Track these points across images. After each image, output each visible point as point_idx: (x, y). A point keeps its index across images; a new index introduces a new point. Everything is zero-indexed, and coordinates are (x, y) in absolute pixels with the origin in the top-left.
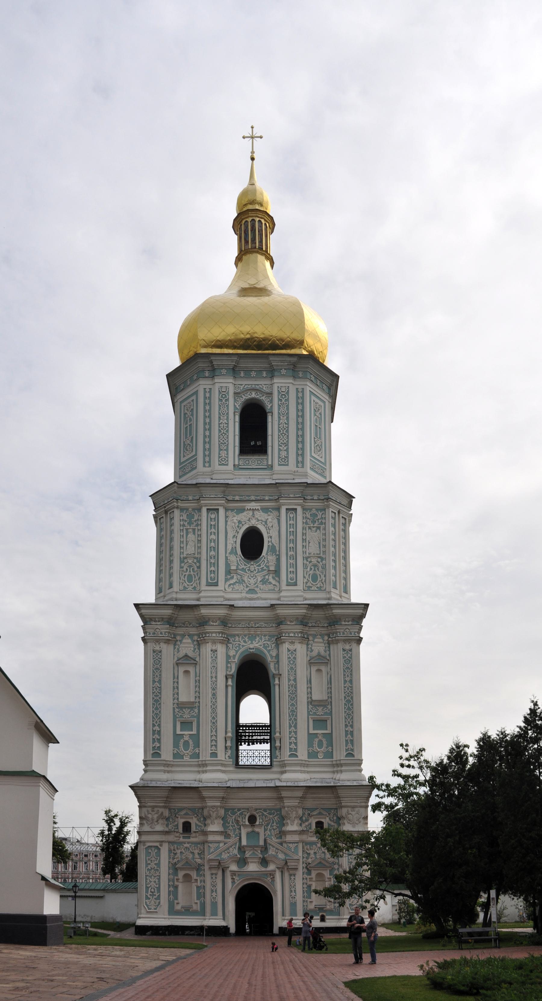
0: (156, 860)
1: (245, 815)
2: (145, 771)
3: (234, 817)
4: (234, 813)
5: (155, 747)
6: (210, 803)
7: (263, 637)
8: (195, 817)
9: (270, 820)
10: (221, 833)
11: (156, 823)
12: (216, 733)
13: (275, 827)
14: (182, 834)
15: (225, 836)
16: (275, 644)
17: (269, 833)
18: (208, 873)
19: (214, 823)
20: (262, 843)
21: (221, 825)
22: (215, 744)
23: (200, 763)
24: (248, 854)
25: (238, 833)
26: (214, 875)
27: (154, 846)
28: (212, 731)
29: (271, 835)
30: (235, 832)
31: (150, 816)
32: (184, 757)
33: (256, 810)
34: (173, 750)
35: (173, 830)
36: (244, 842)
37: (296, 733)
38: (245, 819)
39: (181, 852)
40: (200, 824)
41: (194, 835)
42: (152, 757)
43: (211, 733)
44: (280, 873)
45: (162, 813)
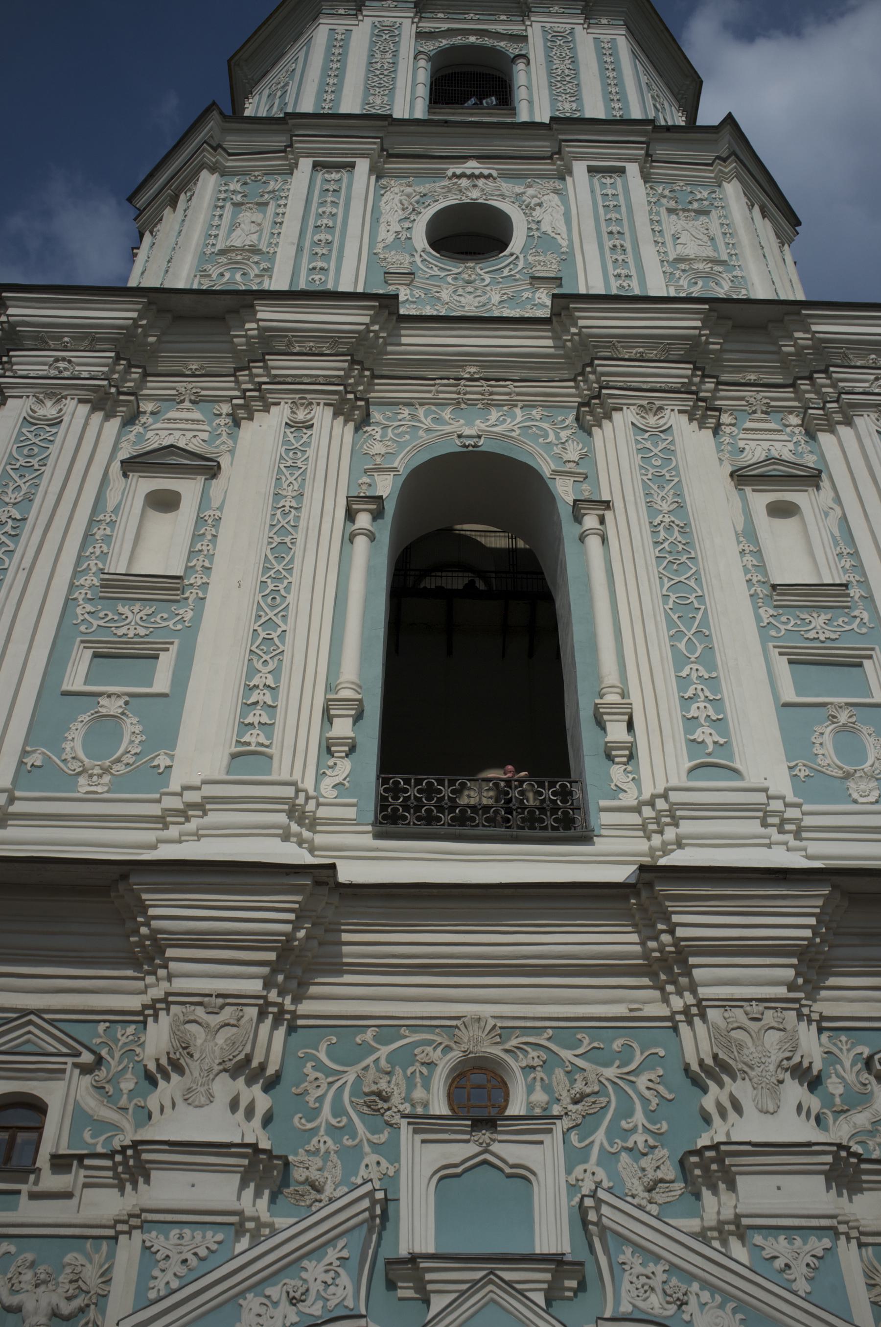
1: (431, 1065)
3: (351, 1078)
7: (518, 411)
8: (85, 1070)
12: (277, 679)
13: (640, 1139)
16: (569, 432)
17: (601, 1174)
19: (211, 1098)
22: (265, 719)
28: (252, 671)
30: (351, 1169)
34: (25, 753)
37: (713, 682)
38: (427, 1087)
40: (108, 1114)
41: (50, 1181)
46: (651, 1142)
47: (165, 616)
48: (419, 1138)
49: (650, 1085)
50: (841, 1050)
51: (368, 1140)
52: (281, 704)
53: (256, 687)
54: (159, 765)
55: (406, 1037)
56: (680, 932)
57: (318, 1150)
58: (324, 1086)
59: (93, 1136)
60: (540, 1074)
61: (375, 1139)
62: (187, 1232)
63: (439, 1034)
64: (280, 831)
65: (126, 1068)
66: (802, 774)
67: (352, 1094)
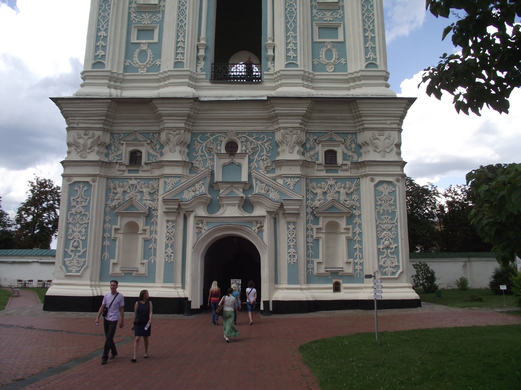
0: (85, 201)
1: (221, 141)
2: (82, 86)
3: (205, 144)
4: (204, 139)
5: (98, 55)
6: (169, 124)
8: (149, 144)
9: (257, 147)
10: (183, 164)
11: (91, 150)
12: (184, 39)
13: (264, 157)
14: (127, 166)
15: (190, 170)
17: (256, 165)
18: (161, 219)
20: (244, 178)
21: (186, 155)
22: (182, 51)
23: (160, 76)
24: (223, 193)
25: (210, 165)
26: (170, 223)
27: (83, 182)
28: (178, 37)
29: (259, 168)
31: (81, 141)
32: (139, 69)
33: (237, 134)
35: (115, 161)
36: (218, 178)
38: (221, 146)
39: (125, 192)
40: (154, 153)
41: (146, 168)
42: (93, 68)
43: (177, 38)
44: (272, 221)
45: (99, 137)
46: (267, 158)
47: (155, 17)
48: (219, 158)
49: (268, 145)
50: (311, 137)
51: (209, 158)
52: (186, 46)
53: (179, 41)
54: (157, 65)
55: (216, 135)
56: (276, 112)
57: (198, 160)
58: (199, 146)
59: (152, 158)
60: (245, 143)
61: (209, 157)
62: (172, 178)
63: (223, 134)
64: (187, 84)
65: (157, 143)
66: (316, 63)
67: (205, 148)
